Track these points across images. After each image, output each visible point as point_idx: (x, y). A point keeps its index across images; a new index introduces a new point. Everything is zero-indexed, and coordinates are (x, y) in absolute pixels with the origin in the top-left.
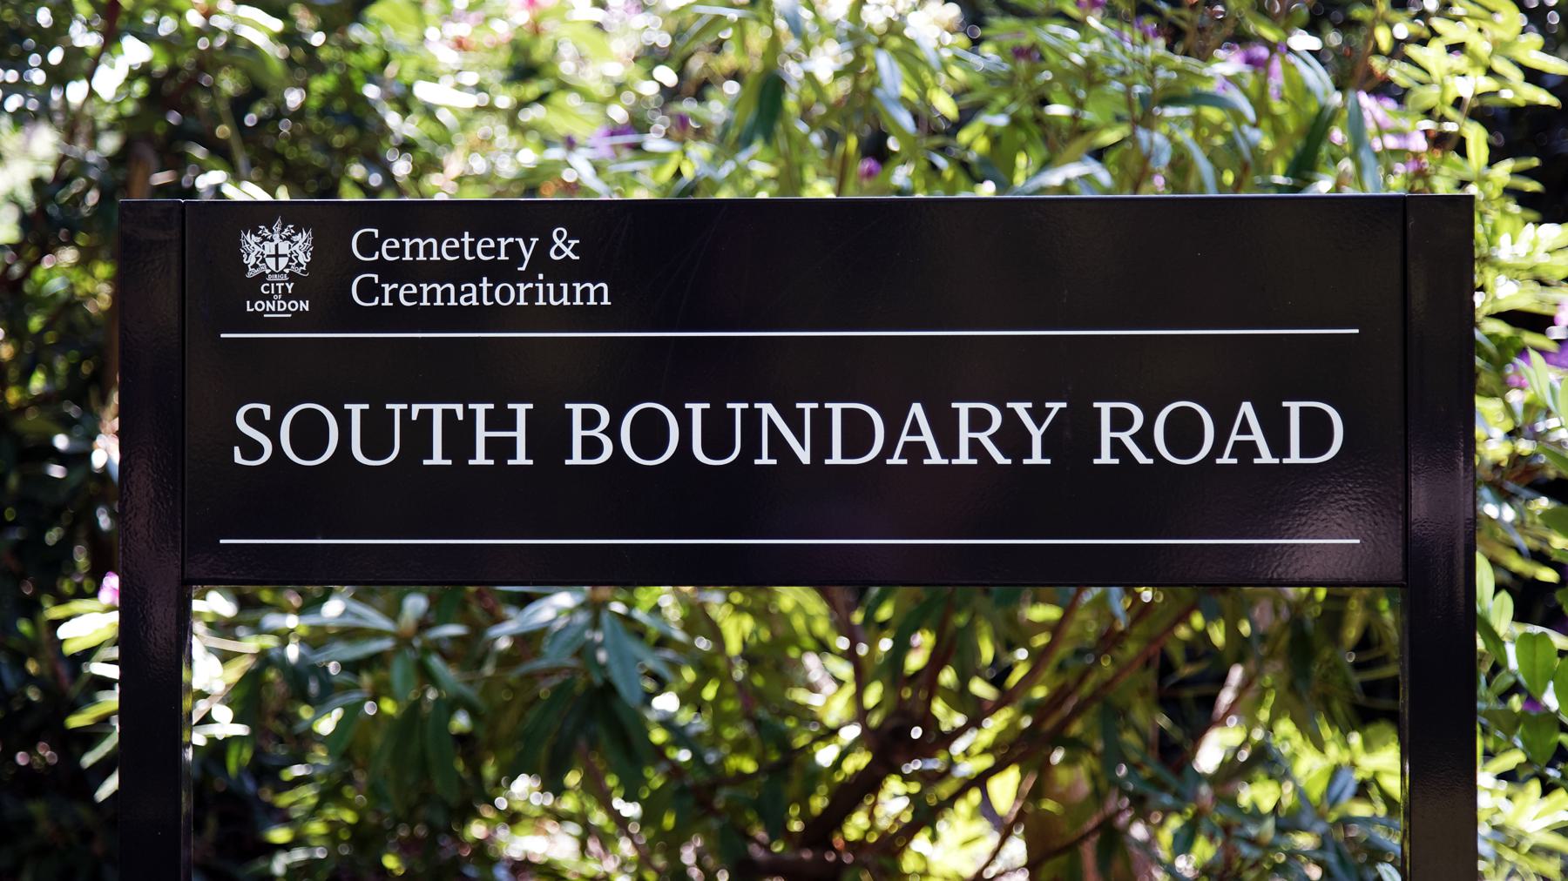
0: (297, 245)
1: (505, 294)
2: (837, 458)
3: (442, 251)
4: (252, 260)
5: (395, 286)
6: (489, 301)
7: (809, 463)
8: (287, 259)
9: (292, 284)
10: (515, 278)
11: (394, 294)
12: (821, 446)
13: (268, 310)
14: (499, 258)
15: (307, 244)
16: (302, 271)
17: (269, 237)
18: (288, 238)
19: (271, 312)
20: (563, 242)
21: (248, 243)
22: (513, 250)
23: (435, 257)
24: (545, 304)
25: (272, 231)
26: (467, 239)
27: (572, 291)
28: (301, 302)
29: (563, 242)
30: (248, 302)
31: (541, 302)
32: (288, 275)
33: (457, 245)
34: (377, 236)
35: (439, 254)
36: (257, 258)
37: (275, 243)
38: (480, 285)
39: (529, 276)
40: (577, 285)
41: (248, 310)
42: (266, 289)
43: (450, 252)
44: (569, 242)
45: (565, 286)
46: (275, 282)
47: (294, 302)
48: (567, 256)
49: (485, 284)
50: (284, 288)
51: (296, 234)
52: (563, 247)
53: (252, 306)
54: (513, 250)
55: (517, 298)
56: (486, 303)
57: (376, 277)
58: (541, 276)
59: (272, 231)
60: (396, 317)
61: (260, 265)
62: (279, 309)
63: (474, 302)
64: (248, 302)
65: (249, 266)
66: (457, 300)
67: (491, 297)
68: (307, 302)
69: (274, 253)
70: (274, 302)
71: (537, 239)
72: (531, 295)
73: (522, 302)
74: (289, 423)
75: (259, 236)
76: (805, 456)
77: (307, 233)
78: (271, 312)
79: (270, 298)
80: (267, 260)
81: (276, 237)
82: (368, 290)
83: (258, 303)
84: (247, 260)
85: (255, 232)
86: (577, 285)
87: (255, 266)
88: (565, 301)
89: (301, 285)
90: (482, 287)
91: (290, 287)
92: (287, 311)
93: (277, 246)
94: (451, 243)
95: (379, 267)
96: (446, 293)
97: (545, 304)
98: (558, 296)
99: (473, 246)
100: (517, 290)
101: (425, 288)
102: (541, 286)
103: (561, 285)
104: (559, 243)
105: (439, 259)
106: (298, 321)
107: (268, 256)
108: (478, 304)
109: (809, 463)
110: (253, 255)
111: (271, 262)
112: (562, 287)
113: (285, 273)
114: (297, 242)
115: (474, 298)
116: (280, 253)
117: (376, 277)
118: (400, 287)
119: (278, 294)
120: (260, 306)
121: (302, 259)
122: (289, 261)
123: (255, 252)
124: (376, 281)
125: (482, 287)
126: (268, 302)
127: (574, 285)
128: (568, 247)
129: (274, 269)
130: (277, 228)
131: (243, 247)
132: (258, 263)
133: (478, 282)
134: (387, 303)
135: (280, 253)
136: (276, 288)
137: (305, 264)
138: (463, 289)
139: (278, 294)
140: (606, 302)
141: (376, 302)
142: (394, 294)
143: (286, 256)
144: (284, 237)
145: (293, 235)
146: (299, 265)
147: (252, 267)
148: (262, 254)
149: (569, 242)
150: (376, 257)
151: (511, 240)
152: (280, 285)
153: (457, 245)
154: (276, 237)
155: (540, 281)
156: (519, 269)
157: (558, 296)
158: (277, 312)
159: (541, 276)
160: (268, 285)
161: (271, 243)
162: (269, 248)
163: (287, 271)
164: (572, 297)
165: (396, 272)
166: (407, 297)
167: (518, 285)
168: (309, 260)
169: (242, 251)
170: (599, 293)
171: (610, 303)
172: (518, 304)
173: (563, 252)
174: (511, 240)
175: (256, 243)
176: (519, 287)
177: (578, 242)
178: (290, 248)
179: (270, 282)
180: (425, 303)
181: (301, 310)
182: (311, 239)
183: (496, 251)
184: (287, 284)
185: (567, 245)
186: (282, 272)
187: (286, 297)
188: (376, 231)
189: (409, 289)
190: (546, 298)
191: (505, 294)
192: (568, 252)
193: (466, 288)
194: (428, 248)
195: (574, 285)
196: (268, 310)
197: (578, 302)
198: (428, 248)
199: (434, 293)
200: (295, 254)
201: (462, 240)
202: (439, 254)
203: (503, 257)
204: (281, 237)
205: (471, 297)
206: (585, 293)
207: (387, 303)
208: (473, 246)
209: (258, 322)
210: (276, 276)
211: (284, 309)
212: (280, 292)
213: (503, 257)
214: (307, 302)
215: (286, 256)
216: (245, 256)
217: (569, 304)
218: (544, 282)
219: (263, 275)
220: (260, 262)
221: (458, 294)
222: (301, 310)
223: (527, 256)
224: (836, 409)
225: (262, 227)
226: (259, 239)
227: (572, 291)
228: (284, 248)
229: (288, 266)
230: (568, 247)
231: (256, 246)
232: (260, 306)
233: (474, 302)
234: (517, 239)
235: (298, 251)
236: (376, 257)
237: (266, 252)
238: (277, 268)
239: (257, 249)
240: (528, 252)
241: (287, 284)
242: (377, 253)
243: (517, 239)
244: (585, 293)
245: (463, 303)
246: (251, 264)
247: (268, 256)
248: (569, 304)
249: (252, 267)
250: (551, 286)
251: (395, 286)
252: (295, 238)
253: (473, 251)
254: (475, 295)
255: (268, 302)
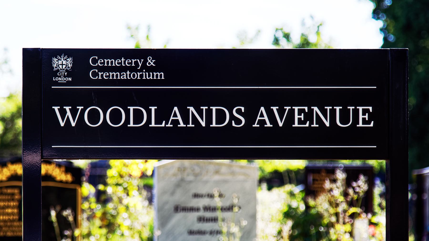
0: (68, 62)
1: (134, 76)
2: (214, 125)
3: (116, 63)
4: (55, 66)
5: (102, 73)
6: (129, 78)
7: (205, 126)
8: (65, 66)
9: (67, 73)
10: (137, 71)
11: (102, 75)
12: (209, 121)
13: (59, 80)
14: (132, 65)
15: (71, 61)
16: (70, 69)
17: (60, 59)
18: (66, 60)
19: (60, 81)
20: (151, 61)
21: (54, 61)
22: (136, 63)
23: (114, 65)
24: (145, 78)
25: (61, 57)
26: (123, 60)
27: (153, 75)
28: (69, 78)
29: (151, 61)
30: (54, 78)
31: (144, 78)
32: (65, 70)
33: (120, 61)
34: (97, 59)
35: (115, 64)
36: (57, 65)
37: (62, 61)
38: (127, 73)
39: (141, 71)
40: (155, 73)
41: (54, 80)
42: (59, 74)
43: (118, 63)
44: (152, 61)
45: (151, 73)
46: (62, 72)
47: (57, 78)
48: (152, 65)
49: (128, 73)
50: (64, 74)
51: (68, 58)
52: (151, 62)
53: (55, 79)
54: (136, 63)
55: (137, 77)
56: (128, 78)
57: (97, 70)
58: (144, 71)
59: (61, 57)
60: (103, 82)
61: (57, 67)
62: (63, 80)
63: (125, 78)
64: (54, 78)
65: (54, 67)
66: (120, 77)
67: (130, 76)
68: (71, 78)
69: (61, 64)
70: (61, 78)
71: (143, 60)
72: (141, 76)
73: (139, 78)
74: (109, 113)
75: (57, 59)
76: (203, 124)
77: (71, 58)
78: (60, 81)
79: (60, 77)
80: (59, 65)
81: (62, 59)
82: (95, 74)
83: (66, 78)
84: (54, 65)
85: (56, 58)
86: (155, 73)
87: (56, 67)
88: (151, 78)
89: (69, 73)
90: (127, 74)
91: (66, 74)
92: (65, 81)
93: (62, 62)
94: (119, 61)
95: (98, 67)
96: (117, 76)
97: (145, 78)
98: (149, 76)
99: (125, 62)
100: (137, 74)
101: (111, 74)
102: (144, 73)
103: (150, 73)
104: (149, 61)
105: (115, 65)
106: (68, 83)
107: (60, 65)
108: (126, 78)
109: (205, 126)
110: (55, 64)
111: (61, 66)
112: (150, 74)
113: (64, 70)
114: (68, 61)
115: (125, 77)
116: (63, 64)
117: (97, 70)
118: (104, 73)
119: (62, 76)
120: (57, 79)
121: (69, 66)
122: (66, 66)
123: (56, 63)
124: (97, 72)
125: (127, 74)
126: (59, 78)
127: (154, 73)
128: (152, 62)
129: (61, 68)
130: (62, 56)
131: (53, 62)
132: (57, 66)
133: (126, 72)
134: (100, 78)
135: (63, 64)
136: (62, 74)
137: (70, 67)
138: (122, 74)
139: (62, 76)
140: (163, 78)
141: (97, 78)
142: (102, 75)
143: (65, 65)
144: (64, 59)
145: (67, 59)
146: (69, 67)
147: (55, 68)
148: (58, 64)
149: (152, 61)
150: (97, 65)
151: (136, 60)
152: (63, 73)
153: (120, 61)
154: (62, 59)
155: (144, 72)
156: (138, 68)
157: (149, 76)
158: (62, 81)
159: (144, 71)
160: (60, 73)
161: (61, 61)
162: (60, 62)
163: (65, 69)
164: (153, 77)
165: (103, 69)
166: (106, 76)
167: (138, 73)
168: (72, 66)
169: (52, 63)
170: (161, 75)
171: (164, 78)
172: (138, 78)
173: (151, 64)
174: (136, 60)
175: (56, 61)
176: (138, 74)
177: (155, 61)
178: (66, 62)
179: (60, 72)
180: (111, 78)
181: (69, 80)
182: (72, 60)
183: (131, 63)
184: (65, 73)
185: (152, 62)
186: (64, 69)
187: (65, 77)
188: (97, 57)
189: (106, 74)
190: (146, 77)
191: (134, 76)
192: (152, 63)
193: (123, 74)
194: (112, 63)
195: (154, 73)
196: (59, 80)
197: (155, 78)
198: (112, 63)
199: (114, 75)
200: (68, 64)
201: (122, 60)
202: (115, 64)
203: (133, 65)
204: (63, 59)
205: (124, 76)
206: (157, 75)
207: (100, 78)
208: (125, 62)
209: (57, 84)
210: (62, 70)
211: (64, 80)
212: (63, 75)
213: (133, 65)
214: (71, 78)
215: (65, 65)
216: (53, 64)
217: (152, 78)
218: (145, 72)
219: (58, 71)
220: (58, 66)
221: (120, 76)
222: (69, 80)
223: (140, 65)
224: (214, 109)
225: (58, 56)
226: (57, 60)
227: (153, 75)
228: (64, 62)
229: (65, 68)
230: (152, 62)
231: (56, 62)
232: (57, 79)
233: (125, 78)
234: (137, 60)
235: (68, 63)
236: (97, 65)
237: (59, 63)
238: (62, 68)
239: (57, 62)
240: (140, 64)
241: (65, 73)
242: (97, 64)
243: (137, 60)
244: (157, 75)
245: (122, 78)
246: (55, 67)
247: (60, 65)
248: (152, 78)
249: (55, 68)
250: (147, 73)
251: (102, 73)
252: (67, 60)
253: (125, 63)
254: (126, 76)
255: (59, 78)
